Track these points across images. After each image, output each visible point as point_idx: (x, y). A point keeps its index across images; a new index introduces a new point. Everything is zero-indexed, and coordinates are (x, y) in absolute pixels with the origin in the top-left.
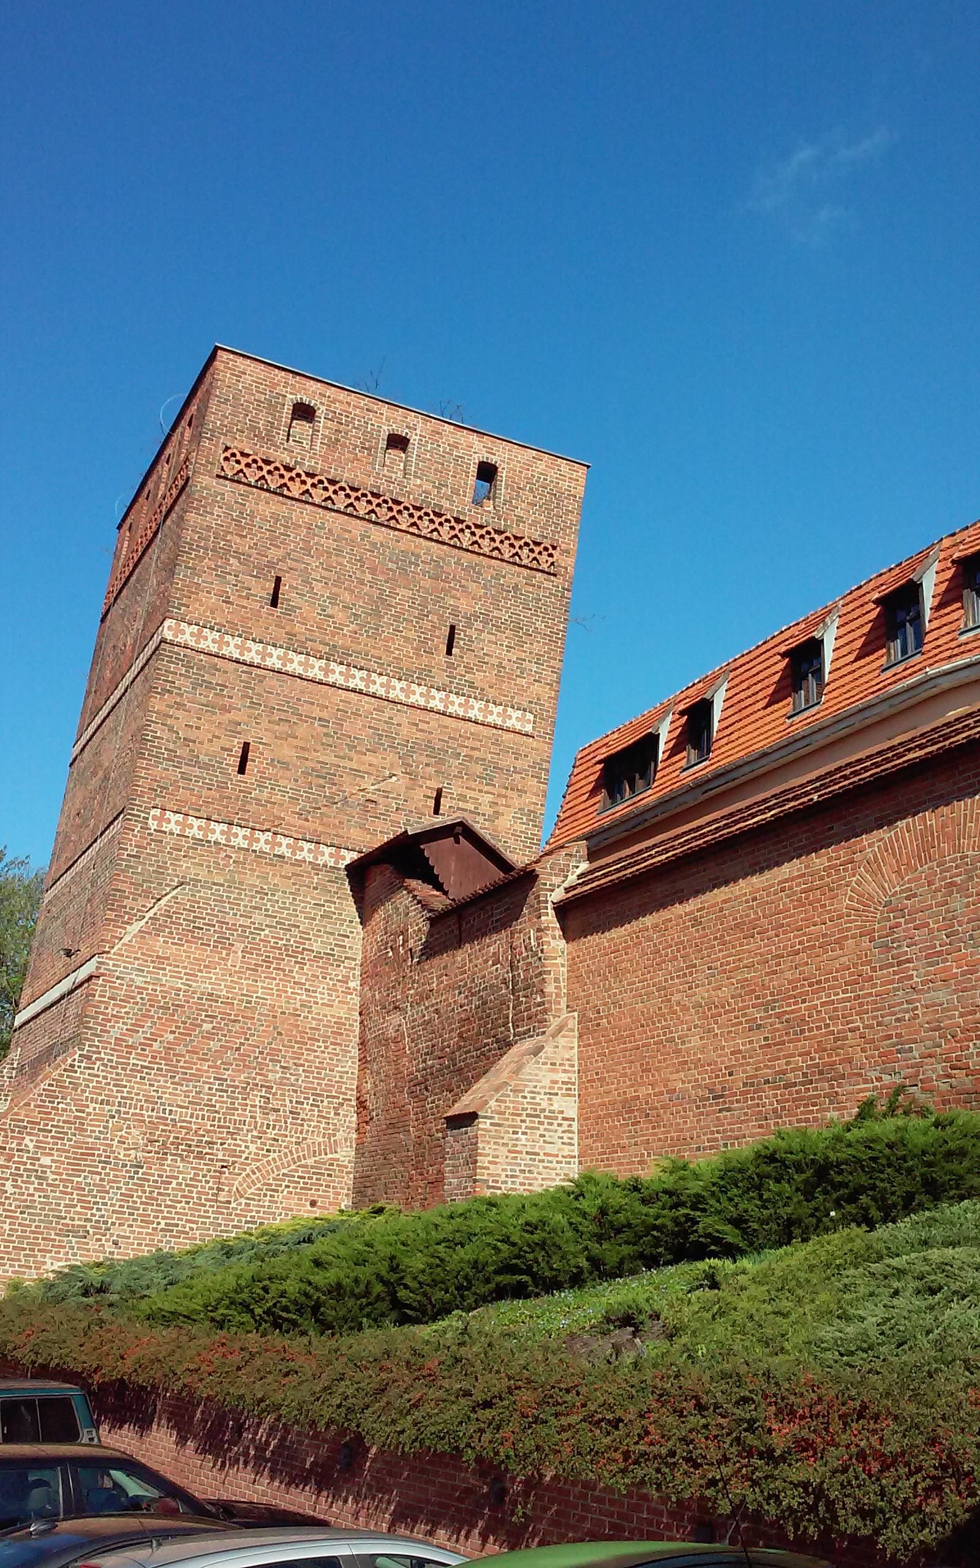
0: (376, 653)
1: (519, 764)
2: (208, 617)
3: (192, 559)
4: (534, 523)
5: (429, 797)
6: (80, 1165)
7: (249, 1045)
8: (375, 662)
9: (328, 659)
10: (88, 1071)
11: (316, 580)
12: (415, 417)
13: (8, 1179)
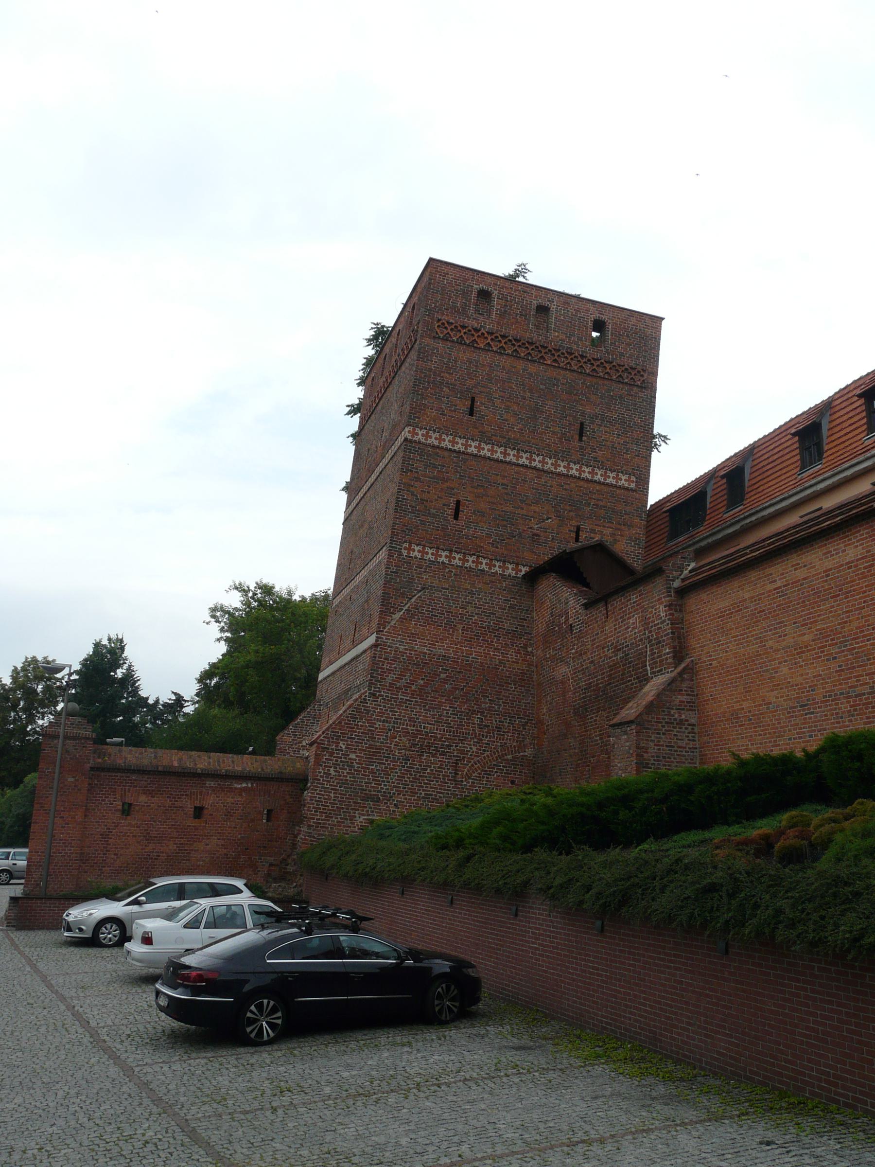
0: (533, 441)
4: (631, 356)
6: (373, 759)
7: (469, 687)
9: (505, 447)
10: (374, 703)
13: (331, 767)
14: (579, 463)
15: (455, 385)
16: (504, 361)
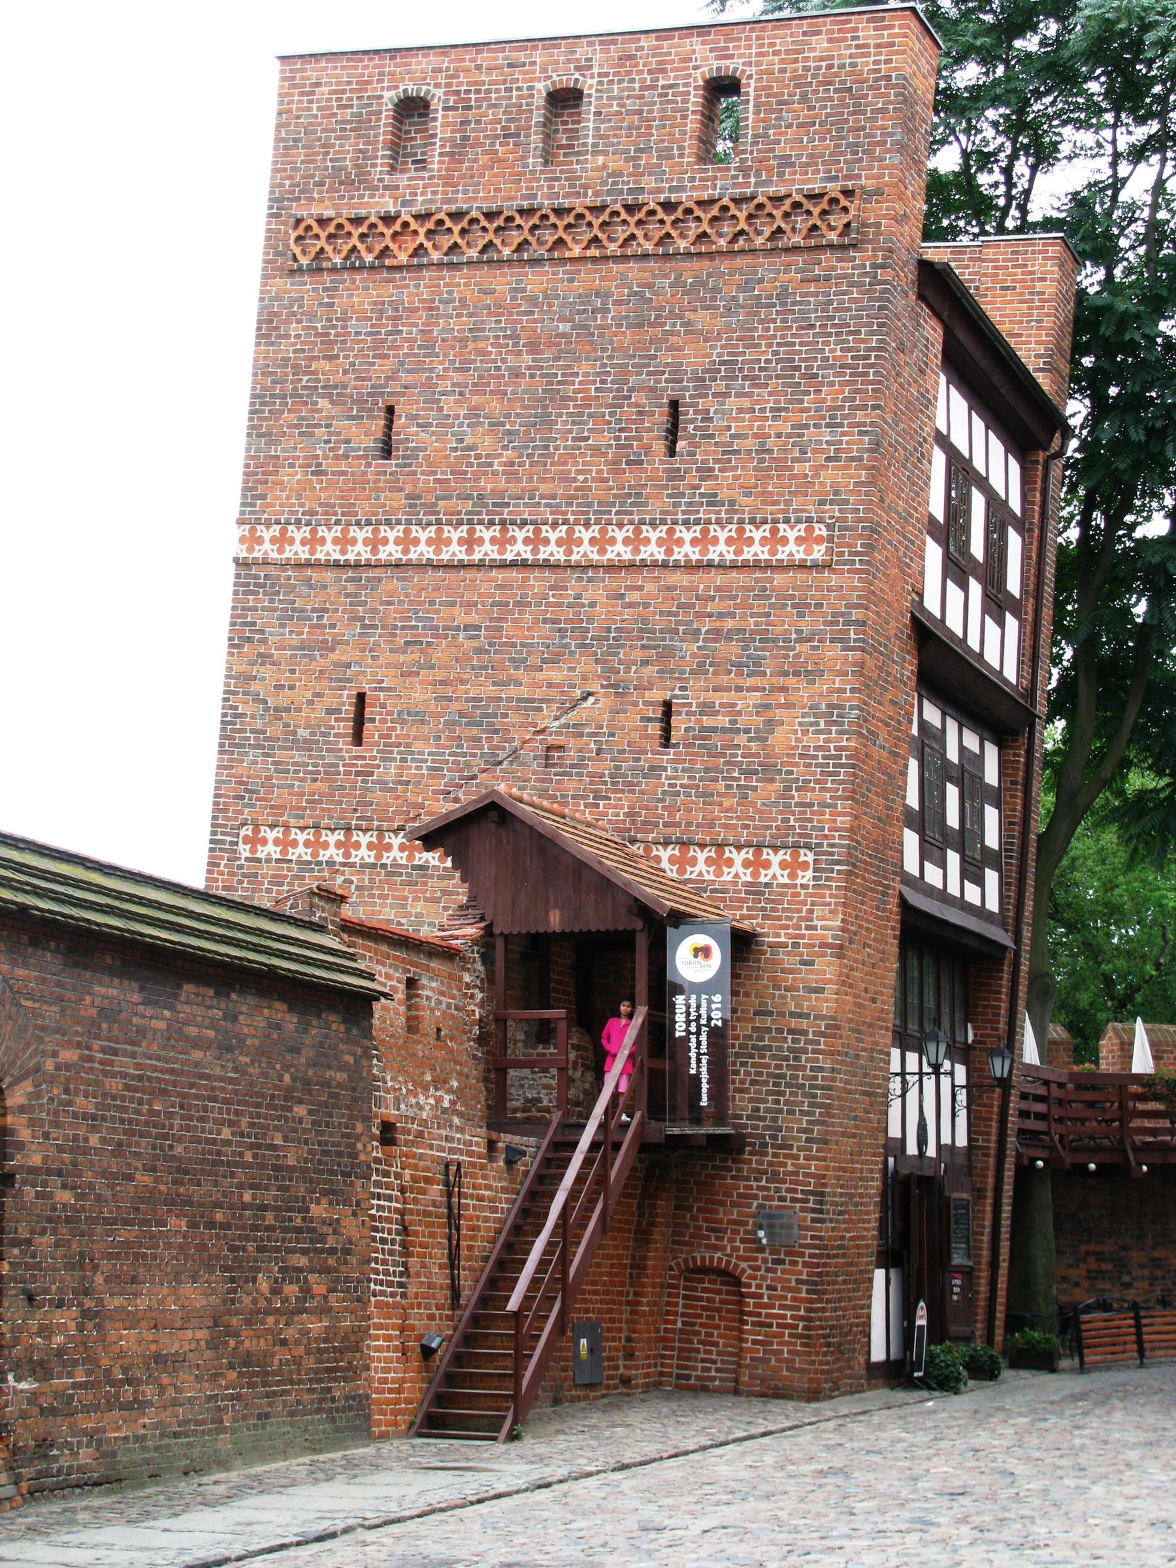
0: (544, 488)
1: (807, 624)
2: (293, 505)
3: (265, 419)
5: (649, 720)
8: (547, 505)
12: (591, 44)
14: (663, 522)
15: (345, 387)
16: (465, 284)
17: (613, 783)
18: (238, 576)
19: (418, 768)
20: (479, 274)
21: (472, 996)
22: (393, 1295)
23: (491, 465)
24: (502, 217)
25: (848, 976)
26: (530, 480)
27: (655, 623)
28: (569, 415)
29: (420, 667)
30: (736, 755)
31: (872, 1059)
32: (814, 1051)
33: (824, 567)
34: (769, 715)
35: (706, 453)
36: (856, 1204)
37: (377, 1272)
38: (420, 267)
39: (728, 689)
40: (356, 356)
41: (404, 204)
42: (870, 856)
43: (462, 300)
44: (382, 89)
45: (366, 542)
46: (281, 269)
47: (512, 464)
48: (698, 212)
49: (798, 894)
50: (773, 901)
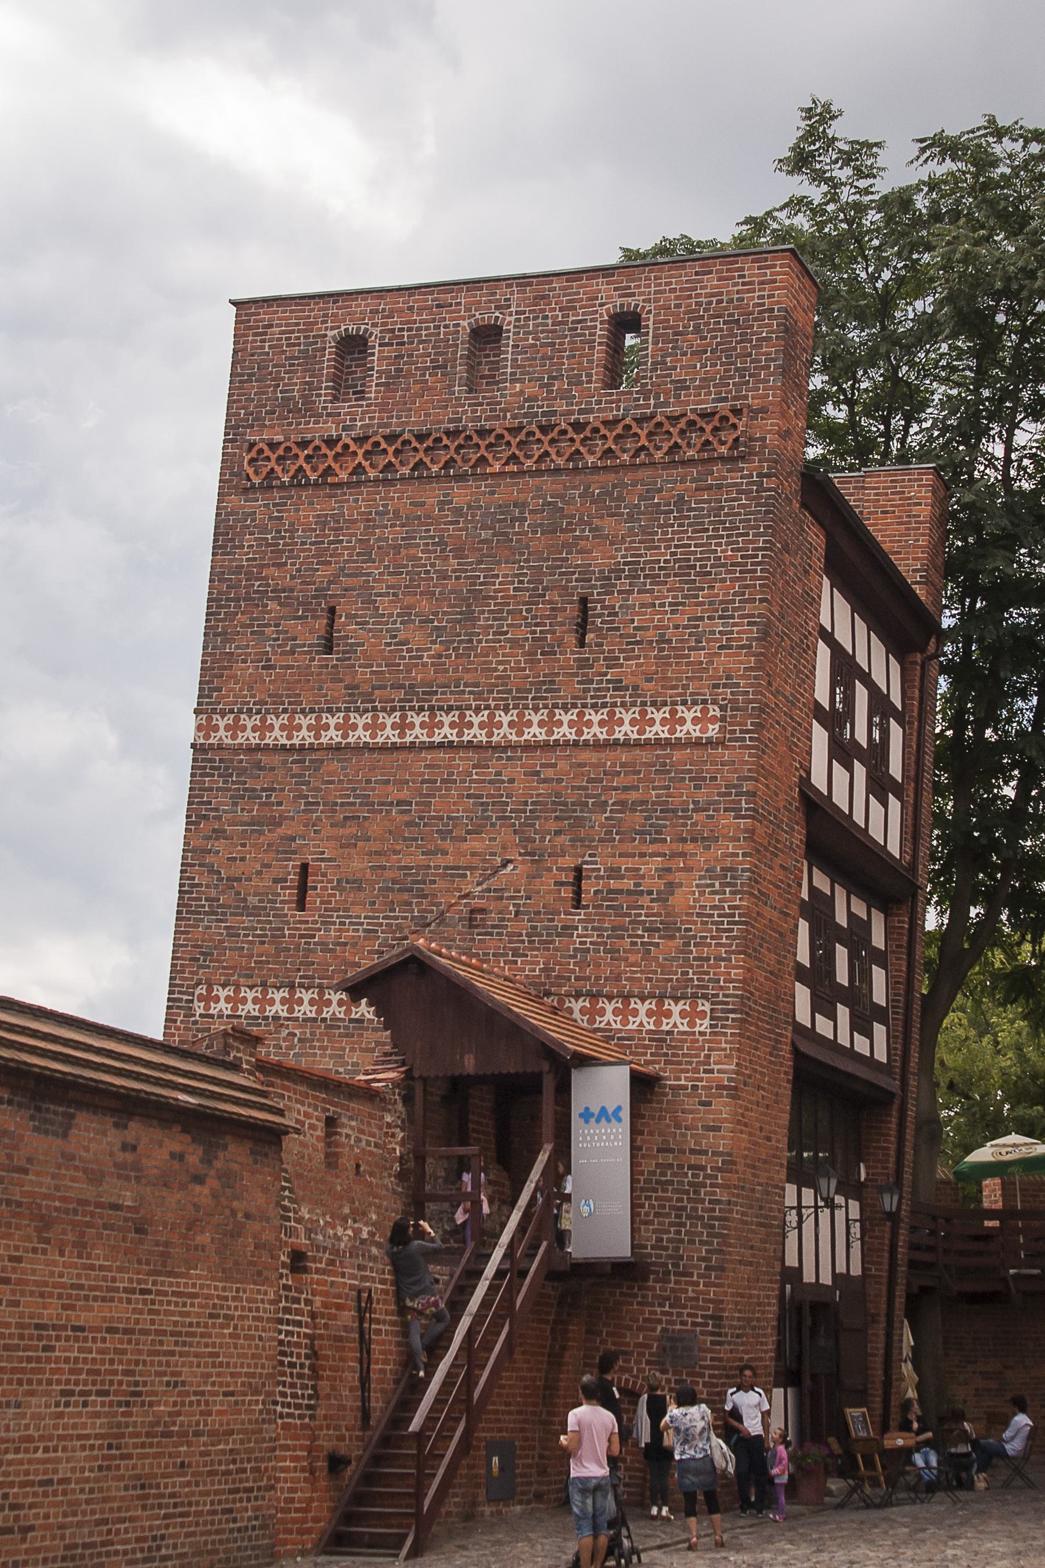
0: (468, 677)
2: (246, 696)
5: (562, 884)
8: (470, 693)
9: (403, 708)
11: (380, 595)
15: (292, 590)
16: (399, 497)
17: (530, 942)
18: (194, 760)
19: (354, 930)
20: (410, 489)
21: (393, 1135)
22: (301, 1417)
23: (421, 657)
24: (431, 438)
25: (743, 1116)
26: (456, 671)
27: (567, 796)
28: (490, 612)
29: (357, 839)
30: (640, 915)
31: (768, 1193)
32: (712, 1185)
33: (717, 744)
34: (670, 877)
35: (611, 644)
36: (754, 1328)
37: (283, 1395)
38: (359, 483)
39: (633, 855)
40: (301, 564)
41: (344, 429)
42: (763, 1007)
43: (396, 512)
44: (326, 329)
45: (310, 728)
46: (235, 487)
47: (440, 656)
48: (603, 431)
49: (697, 1041)
50: (674, 1047)
